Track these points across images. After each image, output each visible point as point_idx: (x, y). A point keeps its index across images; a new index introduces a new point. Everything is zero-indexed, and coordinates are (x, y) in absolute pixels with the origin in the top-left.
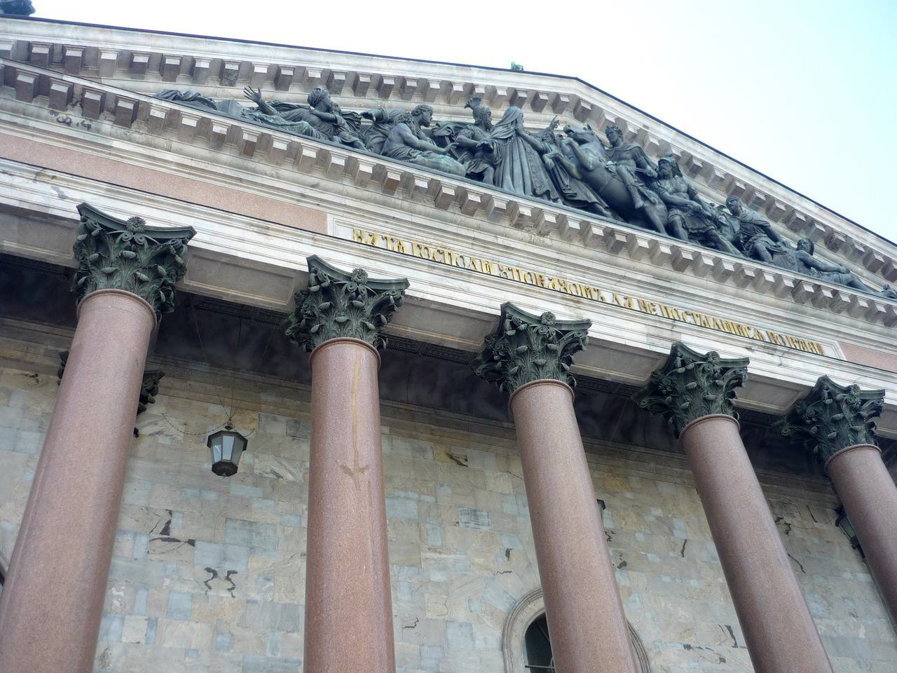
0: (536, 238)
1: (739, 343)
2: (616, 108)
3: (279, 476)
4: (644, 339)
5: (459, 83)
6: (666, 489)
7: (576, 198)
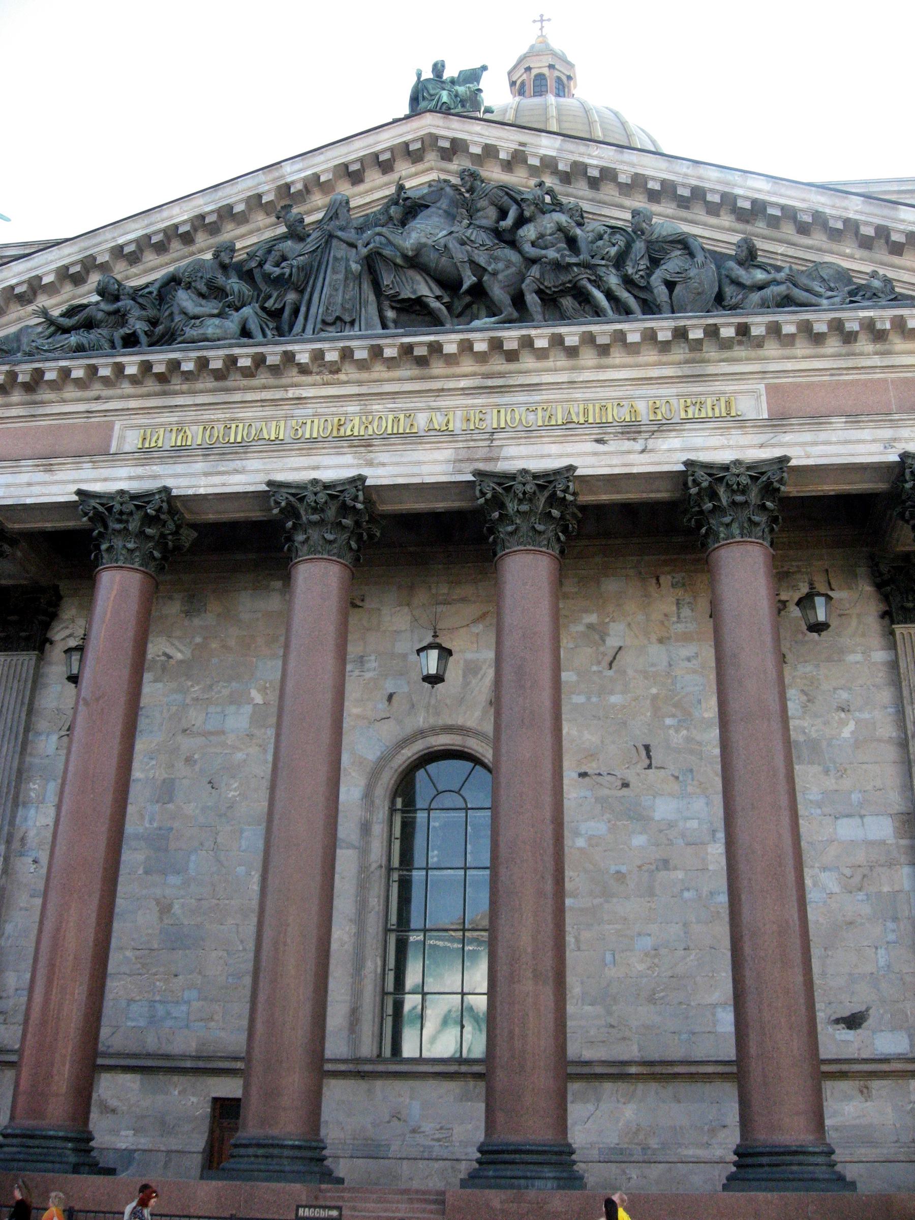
0: (328, 377)
1: (587, 437)
2: (483, 132)
3: (169, 657)
5: (268, 191)
6: (611, 586)
7: (400, 298)
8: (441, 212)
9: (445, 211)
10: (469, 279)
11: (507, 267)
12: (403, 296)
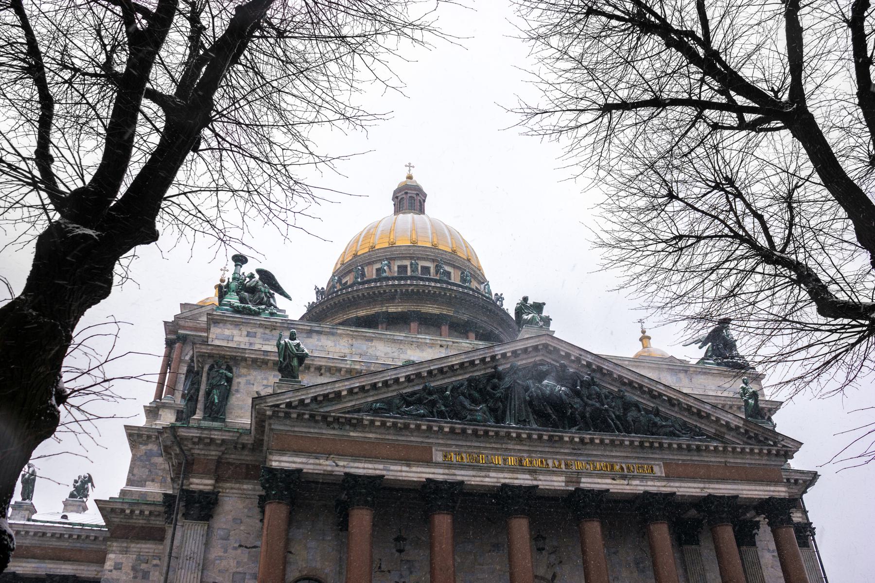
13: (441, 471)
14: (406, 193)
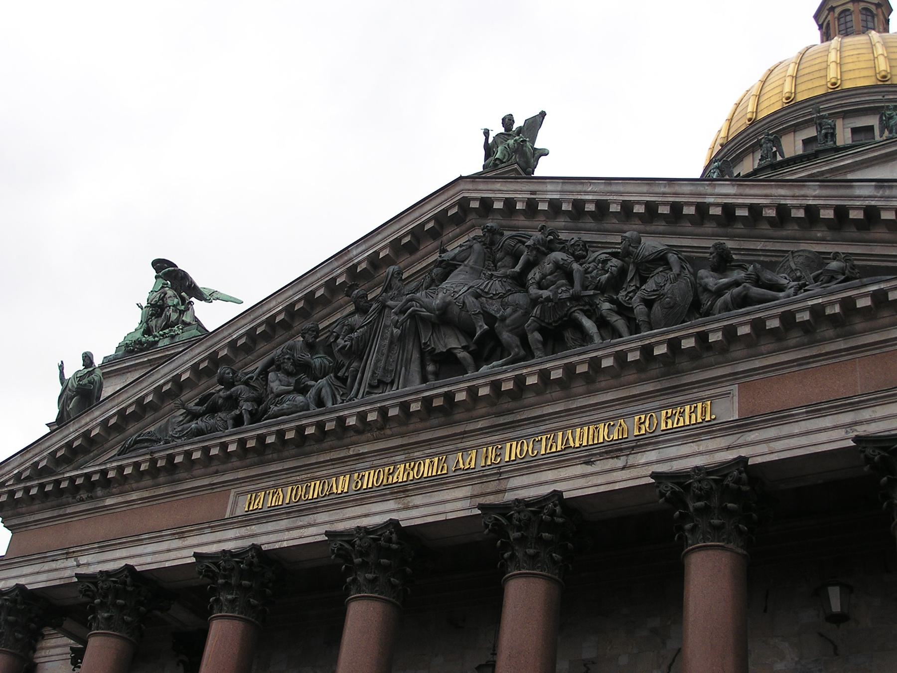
4: (466, 504)
8: (467, 269)
9: (471, 268)
10: (482, 327)
11: (514, 311)
12: (437, 351)
13: (231, 534)
14: (832, 9)
